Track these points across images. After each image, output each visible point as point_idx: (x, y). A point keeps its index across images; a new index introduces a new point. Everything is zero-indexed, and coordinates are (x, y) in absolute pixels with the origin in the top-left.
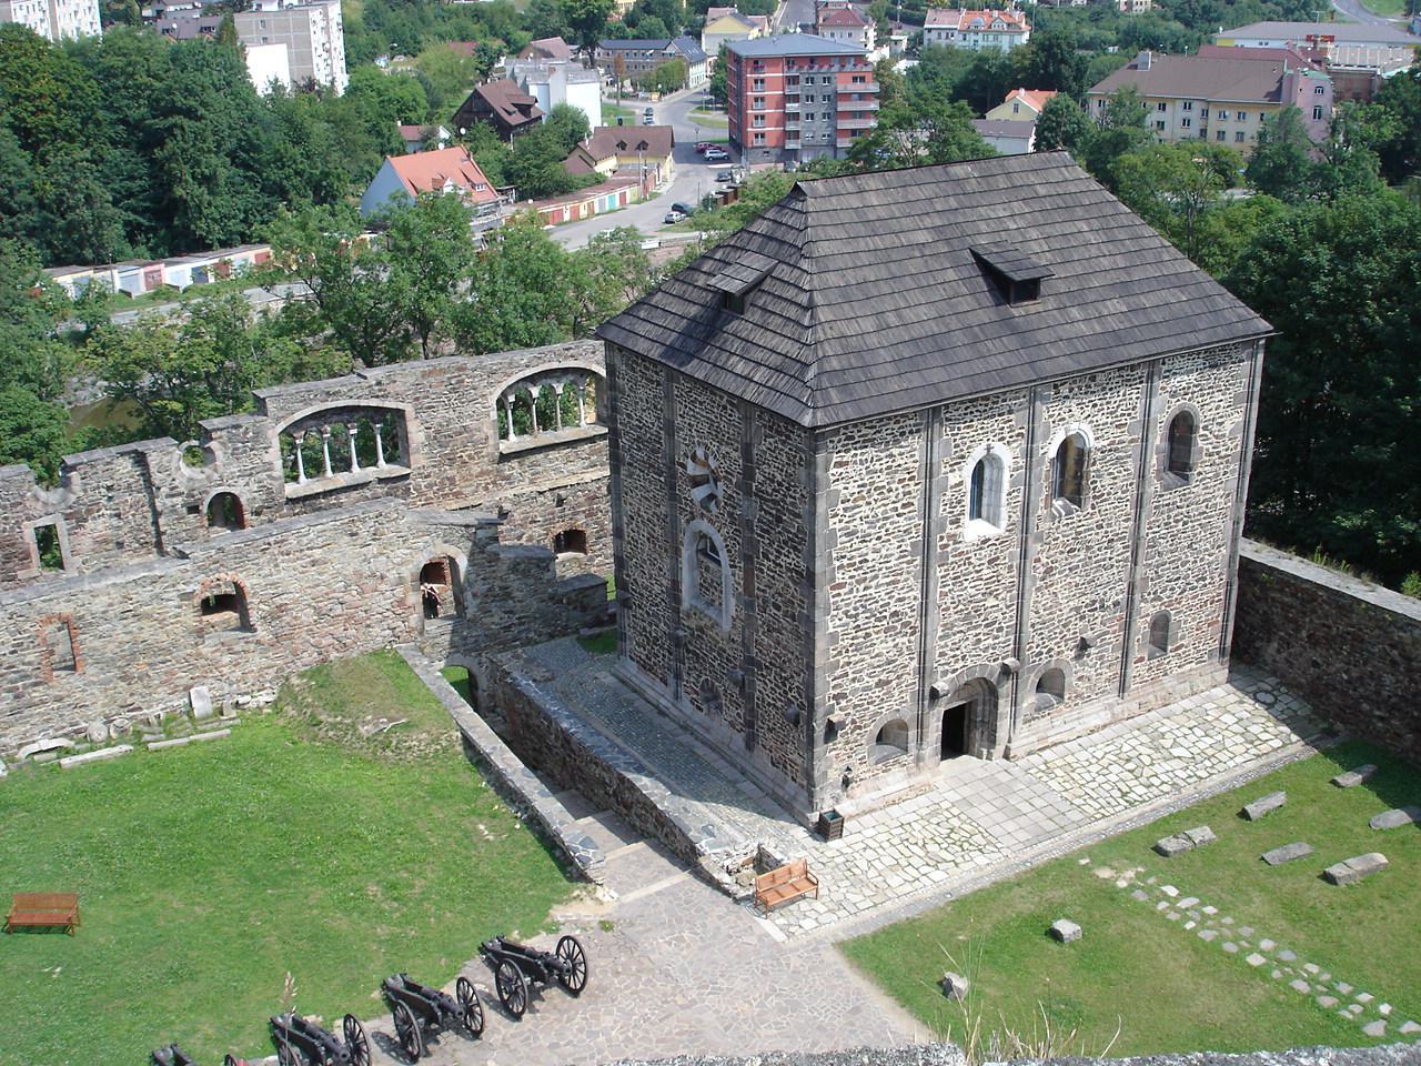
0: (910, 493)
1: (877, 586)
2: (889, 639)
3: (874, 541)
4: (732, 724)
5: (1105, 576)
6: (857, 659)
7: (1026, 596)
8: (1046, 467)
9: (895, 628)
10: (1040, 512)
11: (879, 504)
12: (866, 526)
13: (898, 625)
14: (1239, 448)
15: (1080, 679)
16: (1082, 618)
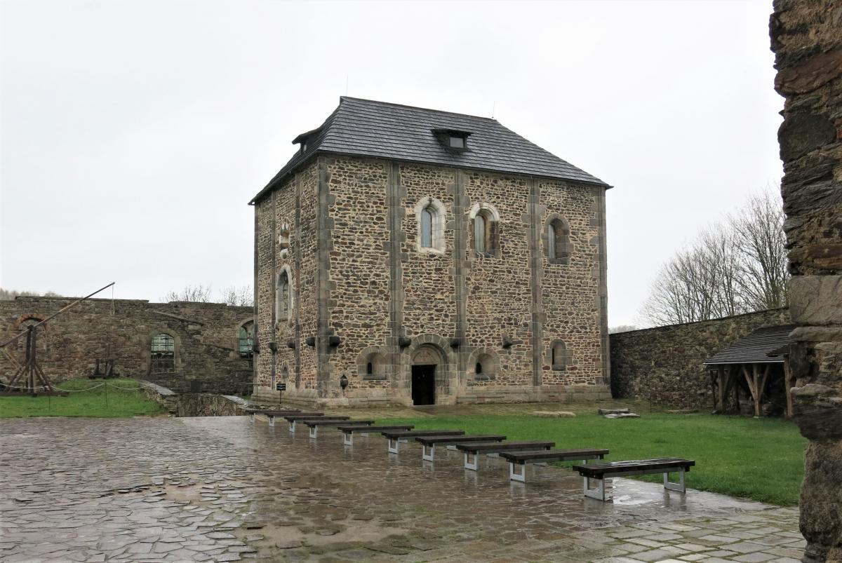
0: (380, 212)
3: (358, 234)
5: (516, 305)
6: (349, 303)
7: (462, 298)
9: (374, 292)
10: (467, 249)
12: (353, 223)
13: (377, 291)
14: (598, 253)
15: (506, 367)
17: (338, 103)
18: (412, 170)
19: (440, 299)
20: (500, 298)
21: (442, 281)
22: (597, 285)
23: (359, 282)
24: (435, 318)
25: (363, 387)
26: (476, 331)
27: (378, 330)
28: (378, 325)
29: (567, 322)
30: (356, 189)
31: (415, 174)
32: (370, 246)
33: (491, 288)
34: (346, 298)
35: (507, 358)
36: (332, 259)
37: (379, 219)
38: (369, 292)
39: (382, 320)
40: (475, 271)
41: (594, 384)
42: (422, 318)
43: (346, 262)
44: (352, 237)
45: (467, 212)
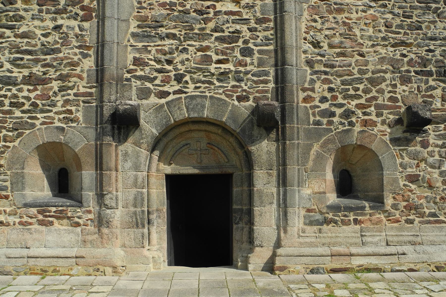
15: (413, 179)
16: (405, 80)
24: (215, 58)
25: (21, 223)
26: (331, 90)
28: (62, 78)
35: (415, 156)
39: (74, 64)
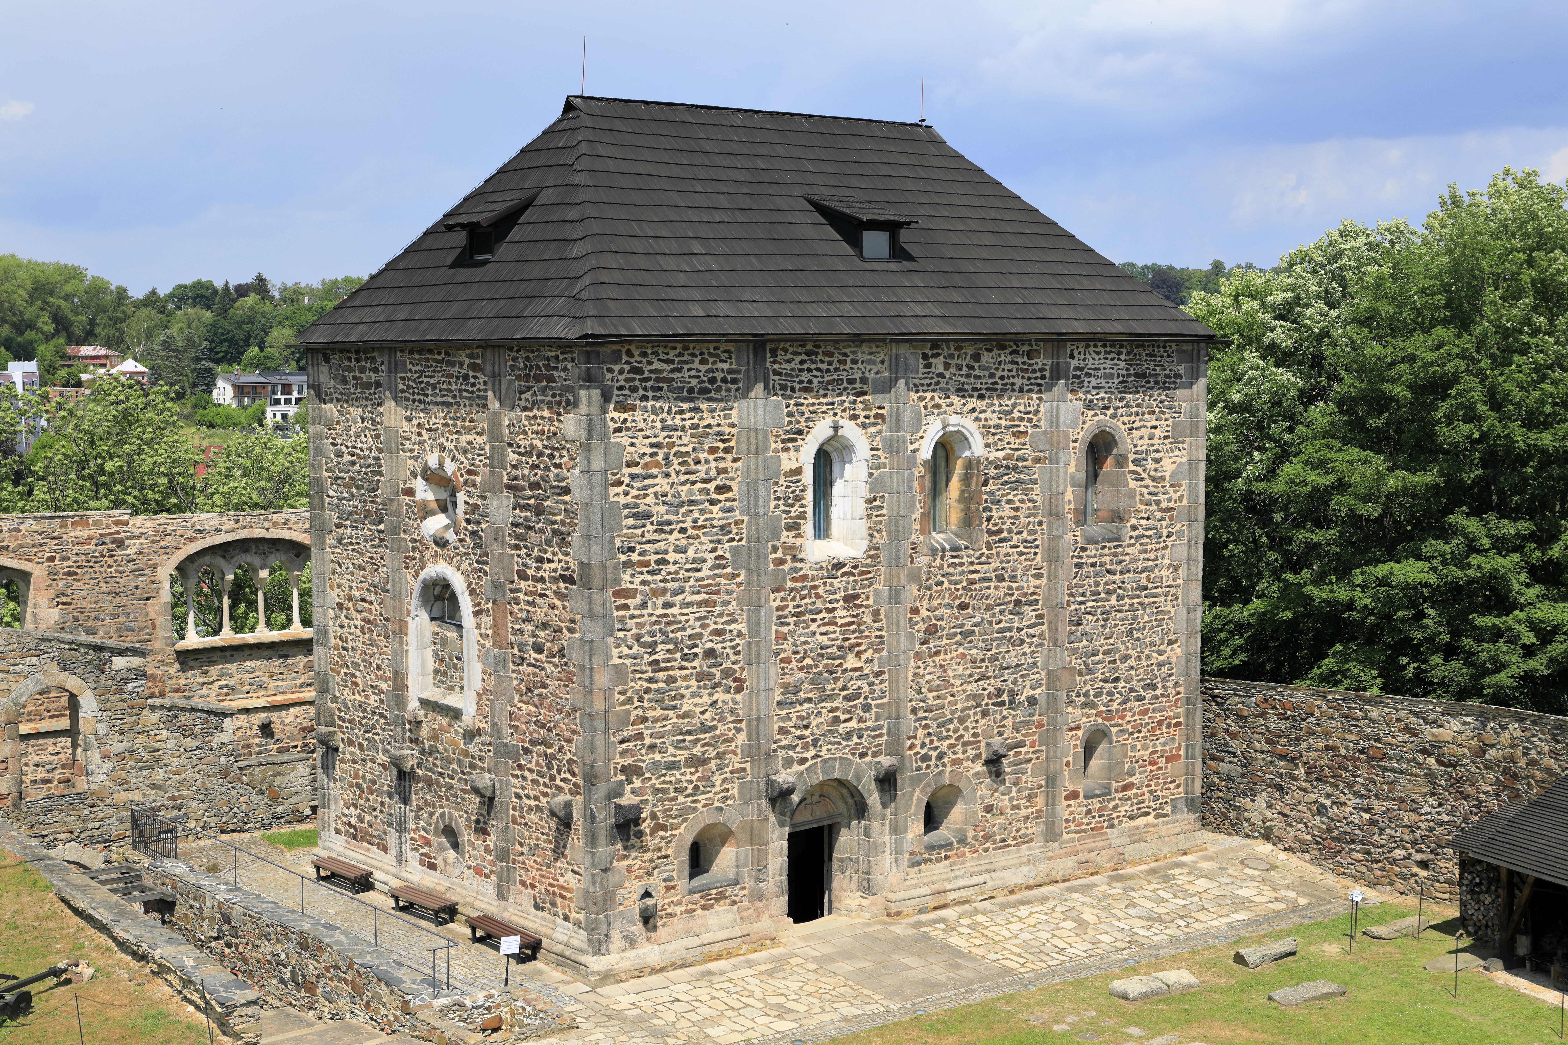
0: (725, 471)
1: (685, 605)
2: (705, 692)
4: (478, 871)
6: (658, 713)
8: (919, 471)
9: (711, 676)
10: (914, 538)
11: (683, 478)
12: (662, 509)
14: (1185, 502)
15: (989, 809)
16: (985, 714)
17: (558, 113)
18: (795, 353)
19: (855, 670)
20: (981, 645)
21: (859, 625)
22: (1180, 582)
23: (678, 655)
24: (843, 717)
27: (720, 768)
29: (1117, 680)
30: (669, 422)
31: (802, 362)
32: (704, 561)
33: (962, 626)
34: (650, 701)
36: (619, 608)
37: (722, 489)
38: (700, 677)
40: (929, 588)
41: (1166, 816)
42: (814, 724)
43: (650, 610)
44: (661, 546)
45: (916, 446)
